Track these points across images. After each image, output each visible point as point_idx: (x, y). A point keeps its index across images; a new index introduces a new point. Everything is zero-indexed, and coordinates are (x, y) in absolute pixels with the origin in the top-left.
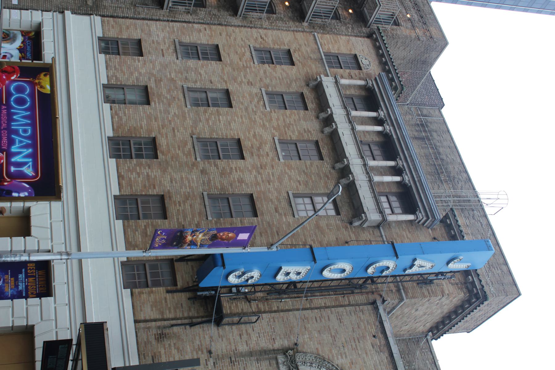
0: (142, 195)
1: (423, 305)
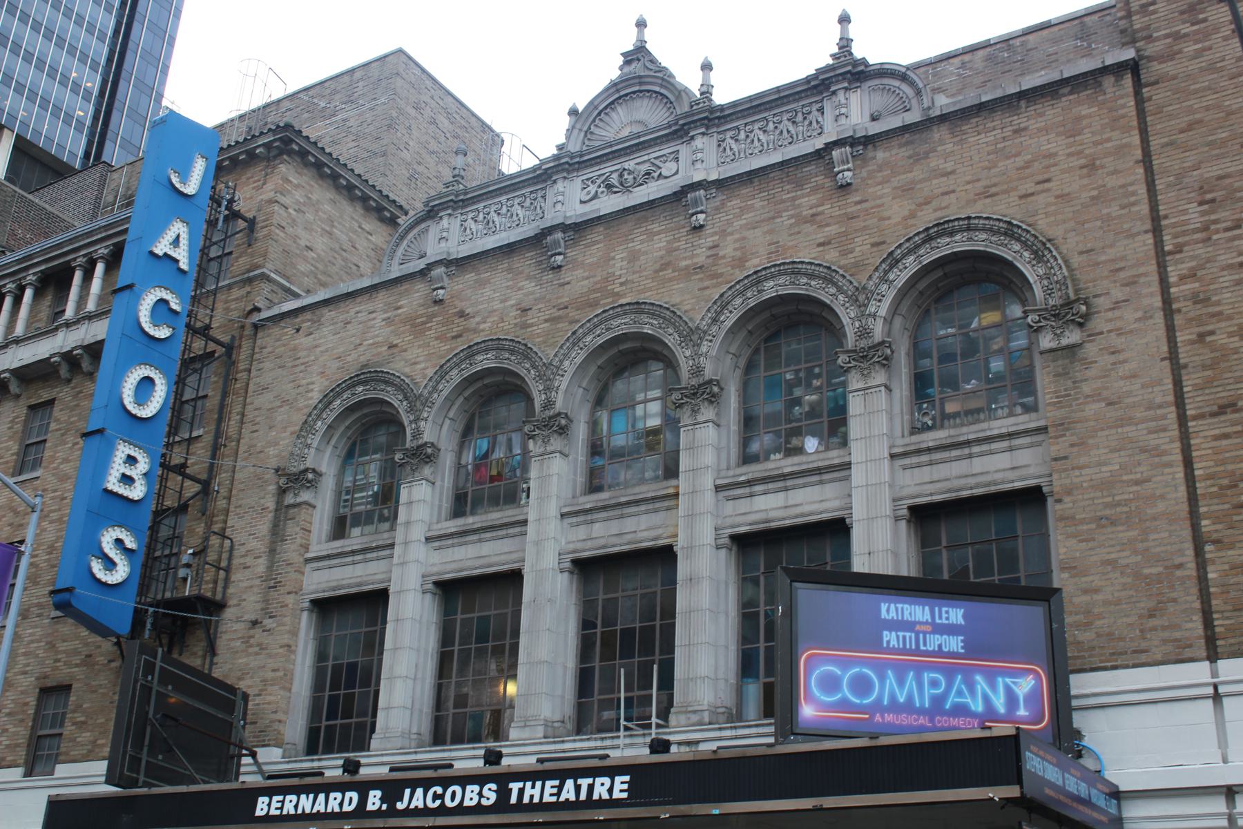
0: (33, 727)
1: (295, 238)
